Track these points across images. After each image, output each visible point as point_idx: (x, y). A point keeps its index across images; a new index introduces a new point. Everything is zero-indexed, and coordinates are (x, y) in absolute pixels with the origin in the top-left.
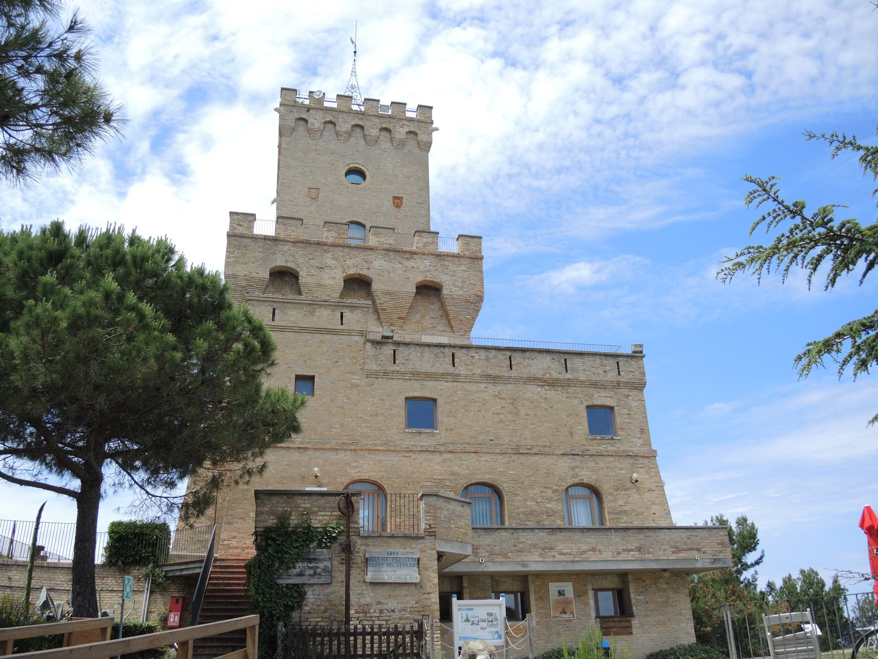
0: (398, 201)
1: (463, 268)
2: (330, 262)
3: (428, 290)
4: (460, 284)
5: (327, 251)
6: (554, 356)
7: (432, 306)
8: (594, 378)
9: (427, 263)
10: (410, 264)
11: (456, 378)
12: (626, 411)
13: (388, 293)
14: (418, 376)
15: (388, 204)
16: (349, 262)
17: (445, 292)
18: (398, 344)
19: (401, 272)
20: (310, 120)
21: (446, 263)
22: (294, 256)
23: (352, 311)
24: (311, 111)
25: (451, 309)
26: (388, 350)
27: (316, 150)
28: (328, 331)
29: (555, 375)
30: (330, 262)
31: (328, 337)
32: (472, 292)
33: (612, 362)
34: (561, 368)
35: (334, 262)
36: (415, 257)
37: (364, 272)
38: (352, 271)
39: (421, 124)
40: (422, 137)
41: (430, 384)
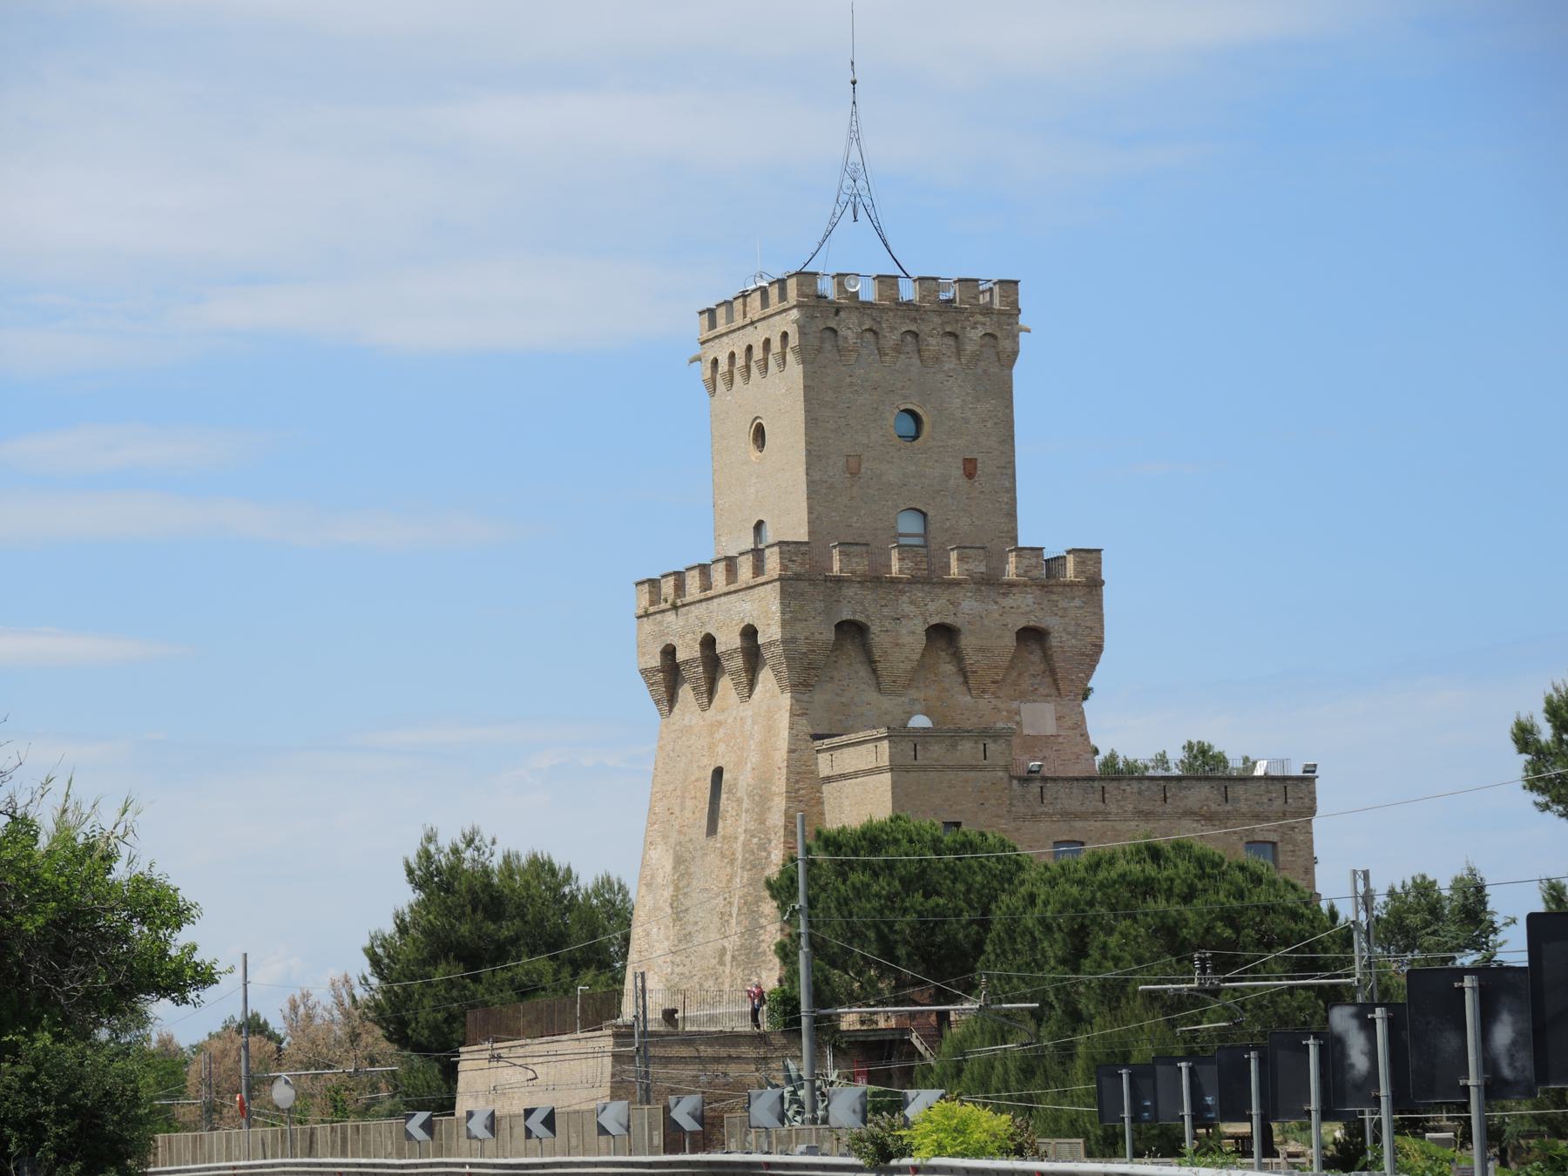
0: (970, 469)
1: (1077, 602)
2: (908, 609)
3: (1032, 636)
4: (1072, 629)
5: (902, 592)
6: (1214, 784)
7: (1032, 657)
8: (1258, 809)
9: (1030, 599)
10: (1008, 602)
11: (1105, 815)
12: (1290, 847)
13: (982, 650)
14: (1067, 815)
15: (957, 472)
16: (932, 607)
17: (1054, 642)
18: (1045, 779)
19: (996, 616)
20: (843, 332)
21: (1055, 597)
22: (862, 604)
23: (995, 741)
24: (842, 314)
25: (1059, 665)
26: (1035, 788)
27: (851, 384)
28: (973, 768)
29: (1214, 807)
30: (908, 609)
31: (972, 774)
32: (1089, 640)
33: (1279, 786)
34: (1220, 798)
35: (912, 608)
36: (1015, 590)
37: (948, 621)
38: (935, 620)
39: (1003, 318)
40: (1006, 344)
41: (1078, 824)
